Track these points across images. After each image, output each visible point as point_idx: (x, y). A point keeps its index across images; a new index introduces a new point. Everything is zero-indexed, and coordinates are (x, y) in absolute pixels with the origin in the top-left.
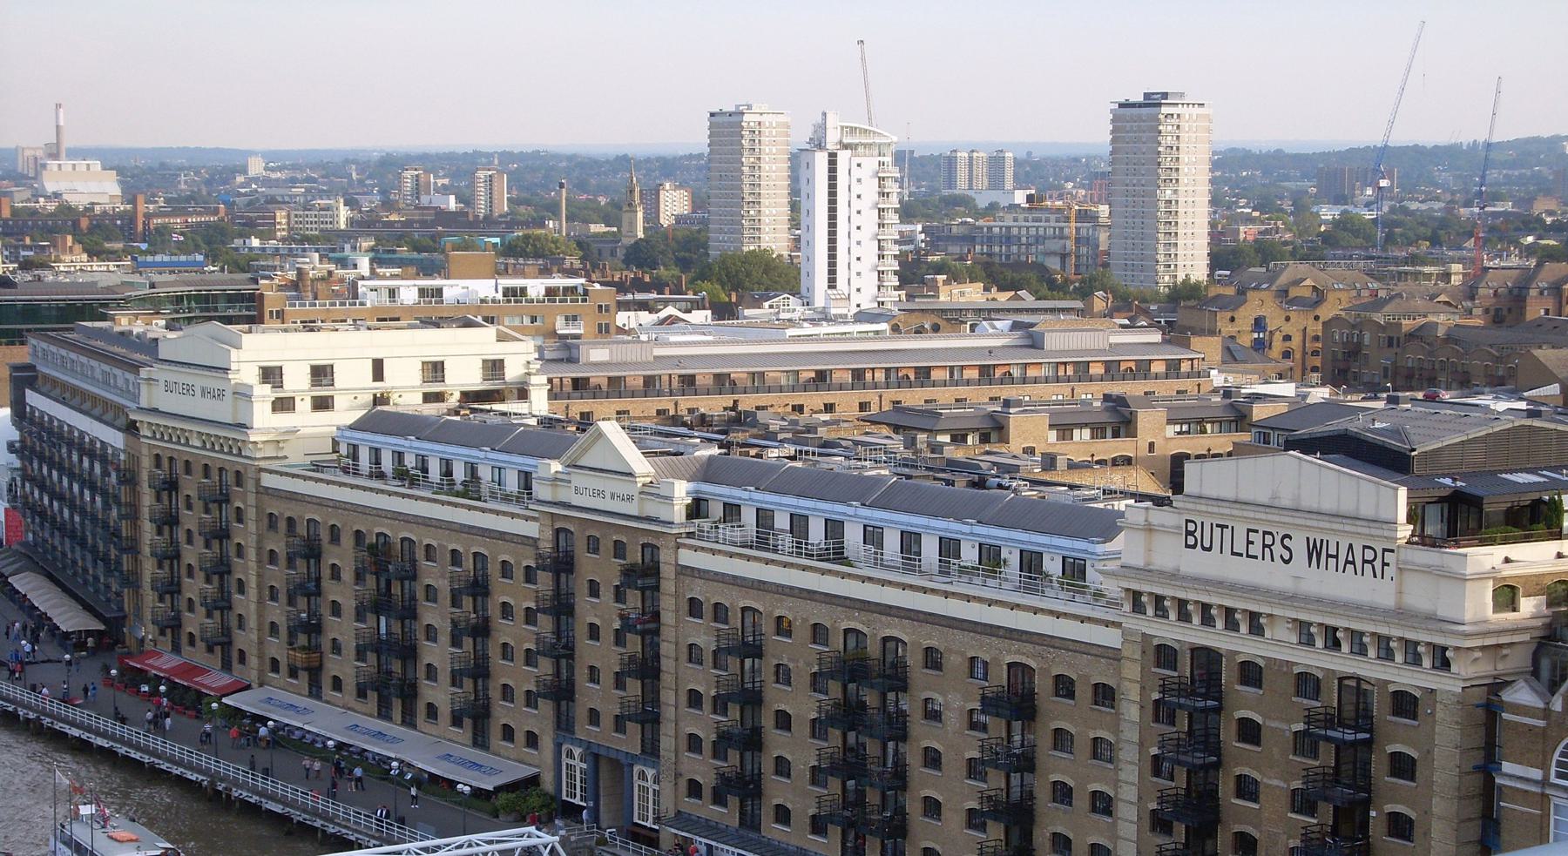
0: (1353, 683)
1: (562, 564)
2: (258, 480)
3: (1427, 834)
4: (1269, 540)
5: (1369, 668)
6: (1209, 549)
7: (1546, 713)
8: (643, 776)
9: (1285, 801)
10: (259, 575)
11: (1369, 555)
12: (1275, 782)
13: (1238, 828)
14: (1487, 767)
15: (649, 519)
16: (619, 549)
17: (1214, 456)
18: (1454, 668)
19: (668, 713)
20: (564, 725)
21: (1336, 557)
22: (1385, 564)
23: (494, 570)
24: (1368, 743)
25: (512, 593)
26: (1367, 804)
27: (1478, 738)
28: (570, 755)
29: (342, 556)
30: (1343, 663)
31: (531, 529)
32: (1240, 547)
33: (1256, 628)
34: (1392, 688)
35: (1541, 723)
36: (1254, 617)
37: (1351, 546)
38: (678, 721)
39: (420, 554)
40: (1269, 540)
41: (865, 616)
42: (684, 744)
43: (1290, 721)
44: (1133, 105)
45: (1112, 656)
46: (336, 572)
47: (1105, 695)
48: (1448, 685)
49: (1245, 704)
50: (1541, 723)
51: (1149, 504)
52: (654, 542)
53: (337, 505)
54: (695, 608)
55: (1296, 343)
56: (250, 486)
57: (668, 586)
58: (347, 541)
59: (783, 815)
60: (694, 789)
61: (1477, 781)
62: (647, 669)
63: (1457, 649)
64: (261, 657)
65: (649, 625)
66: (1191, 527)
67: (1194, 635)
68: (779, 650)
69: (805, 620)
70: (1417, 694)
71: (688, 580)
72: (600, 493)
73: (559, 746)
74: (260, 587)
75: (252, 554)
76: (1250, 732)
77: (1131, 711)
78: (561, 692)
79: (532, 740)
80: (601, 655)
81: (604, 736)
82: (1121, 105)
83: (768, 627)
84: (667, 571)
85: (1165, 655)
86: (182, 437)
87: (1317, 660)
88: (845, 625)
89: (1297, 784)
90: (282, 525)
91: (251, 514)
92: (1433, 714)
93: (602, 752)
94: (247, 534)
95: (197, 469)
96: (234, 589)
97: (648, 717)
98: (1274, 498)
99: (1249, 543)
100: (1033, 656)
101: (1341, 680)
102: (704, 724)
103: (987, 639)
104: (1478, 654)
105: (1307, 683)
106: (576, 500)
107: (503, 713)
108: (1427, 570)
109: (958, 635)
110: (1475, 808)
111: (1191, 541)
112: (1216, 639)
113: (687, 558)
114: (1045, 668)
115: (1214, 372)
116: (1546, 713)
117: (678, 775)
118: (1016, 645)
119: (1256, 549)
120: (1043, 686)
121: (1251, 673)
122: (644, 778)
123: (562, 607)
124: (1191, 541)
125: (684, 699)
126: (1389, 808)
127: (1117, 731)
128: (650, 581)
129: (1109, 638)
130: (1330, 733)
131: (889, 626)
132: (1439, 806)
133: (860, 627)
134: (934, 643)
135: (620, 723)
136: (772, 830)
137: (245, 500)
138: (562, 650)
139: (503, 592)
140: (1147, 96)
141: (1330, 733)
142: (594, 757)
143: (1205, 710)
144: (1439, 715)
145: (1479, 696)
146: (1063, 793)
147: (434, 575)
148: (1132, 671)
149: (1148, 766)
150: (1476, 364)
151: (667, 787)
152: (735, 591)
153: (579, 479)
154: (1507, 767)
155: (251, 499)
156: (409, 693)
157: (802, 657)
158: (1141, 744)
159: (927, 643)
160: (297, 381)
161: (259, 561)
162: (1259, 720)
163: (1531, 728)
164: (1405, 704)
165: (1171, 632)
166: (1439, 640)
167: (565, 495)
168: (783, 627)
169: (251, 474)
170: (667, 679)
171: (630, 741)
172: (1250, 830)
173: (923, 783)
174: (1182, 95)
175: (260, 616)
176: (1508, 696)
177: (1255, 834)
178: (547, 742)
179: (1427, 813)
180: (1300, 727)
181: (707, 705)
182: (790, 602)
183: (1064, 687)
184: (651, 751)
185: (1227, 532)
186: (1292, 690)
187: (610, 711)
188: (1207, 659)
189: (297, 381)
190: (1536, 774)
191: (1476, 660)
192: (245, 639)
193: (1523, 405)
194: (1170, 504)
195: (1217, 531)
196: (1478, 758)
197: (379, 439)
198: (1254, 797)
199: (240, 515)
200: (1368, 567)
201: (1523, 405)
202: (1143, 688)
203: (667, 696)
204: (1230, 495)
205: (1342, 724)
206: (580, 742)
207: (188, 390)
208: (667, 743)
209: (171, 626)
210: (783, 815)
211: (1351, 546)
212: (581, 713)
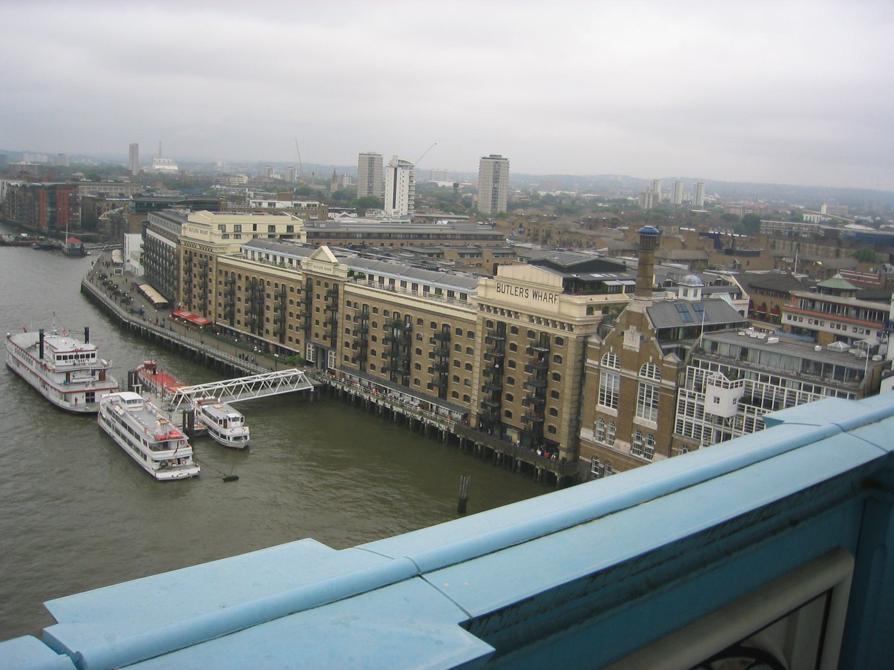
0: (544, 334)
1: (309, 289)
2: (217, 260)
3: (564, 379)
4: (522, 290)
5: (550, 330)
6: (504, 292)
7: (601, 344)
8: (331, 354)
9: (523, 368)
10: (216, 289)
11: (551, 296)
12: (520, 363)
13: (509, 376)
14: (583, 361)
15: (336, 276)
16: (327, 285)
17: (506, 265)
18: (574, 331)
19: (340, 335)
20: (308, 336)
21: (541, 296)
22: (555, 299)
23: (288, 289)
24: (548, 352)
25: (292, 297)
26: (547, 370)
27: (580, 352)
28: (309, 346)
29: (242, 283)
30: (542, 328)
31: (300, 278)
32: (513, 292)
33: (517, 317)
34: (556, 336)
35: (599, 348)
36: (516, 313)
37: (546, 294)
38: (343, 337)
39: (266, 284)
40: (522, 290)
41: (400, 308)
42: (344, 344)
43: (527, 345)
44: (487, 158)
45: (474, 323)
46: (239, 288)
47: (471, 335)
48: (573, 336)
49: (513, 339)
50: (599, 348)
51: (486, 278)
53: (241, 268)
54: (349, 303)
55: (532, 232)
56: (214, 261)
57: (341, 296)
58: (243, 279)
59: (373, 367)
60: (346, 358)
61: (579, 364)
62: (334, 323)
63: (575, 325)
64: (216, 313)
65: (334, 308)
66: (499, 286)
67: (498, 318)
68: (374, 317)
69: (382, 309)
70: (563, 338)
72: (322, 268)
73: (306, 344)
74: (216, 292)
75: (214, 282)
76: (514, 347)
77: (479, 340)
78: (307, 328)
79: (298, 341)
80: (320, 316)
81: (319, 341)
82: (483, 158)
83: (371, 310)
84: (341, 292)
85: (490, 323)
86: (194, 245)
87: (535, 327)
88: (394, 311)
89: (527, 363)
90: (224, 273)
91: (214, 269)
92: (567, 344)
93: (319, 346)
94: (212, 275)
95: (198, 255)
96: (208, 292)
97: (333, 337)
98: (524, 278)
99: (516, 291)
100: (451, 322)
101: (541, 333)
102: (350, 338)
103: (436, 317)
104: (581, 327)
105: (531, 334)
106: (314, 270)
107: (289, 333)
108: (568, 302)
109: (428, 316)
110: (579, 372)
111: (499, 290)
112: (505, 319)
113: (347, 288)
114: (454, 326)
115: (507, 240)
116: (601, 344)
117: (341, 354)
118: (445, 319)
119: (518, 293)
120: (452, 331)
121: (515, 330)
122: (331, 355)
123: (308, 302)
124: (499, 290)
125: (344, 331)
126: (554, 371)
127: (474, 346)
128: (336, 295)
129: (473, 318)
130: (537, 349)
131: (407, 311)
132: (568, 371)
133: (398, 311)
134: (421, 317)
135: (325, 338)
136: (370, 371)
137: (212, 265)
138: (308, 316)
139: (291, 296)
140: (491, 156)
141: (537, 349)
142: (316, 348)
143: (501, 341)
144: (569, 345)
145: (581, 339)
146: (457, 364)
147: (270, 290)
148: (479, 328)
149: (483, 356)
150: (584, 241)
151: (338, 357)
153: (315, 263)
154: (588, 361)
155: (215, 265)
156: (261, 327)
157: (380, 319)
158: (481, 350)
159: (418, 317)
160: (230, 229)
161: (216, 284)
162: (516, 344)
163: (596, 350)
164: (559, 341)
165: (491, 317)
166: (570, 323)
167: (310, 268)
168: (375, 310)
169: (215, 257)
170: (340, 325)
171: (327, 343)
172: (512, 376)
173: (416, 359)
174: (501, 156)
175: (216, 301)
176: (590, 340)
177: (514, 378)
178: (302, 342)
179: (565, 373)
180: (528, 346)
181: (351, 333)
182: (377, 303)
183: (459, 332)
184: (334, 345)
185: (510, 288)
186: (527, 336)
187: (322, 333)
188: (502, 325)
189: (230, 229)
190: (597, 363)
191: (581, 329)
192: (211, 308)
193: (597, 253)
194: (493, 278)
195: (506, 287)
196: (580, 357)
197: (254, 248)
198: (514, 367)
199: (211, 270)
200: (550, 300)
201: (597, 253)
202: (482, 333)
203: (340, 330)
204: (511, 277)
205: (541, 346)
206: (312, 343)
207: (196, 231)
208: (339, 344)
209: (188, 303)
210: (373, 367)
211: (546, 294)
212: (313, 334)
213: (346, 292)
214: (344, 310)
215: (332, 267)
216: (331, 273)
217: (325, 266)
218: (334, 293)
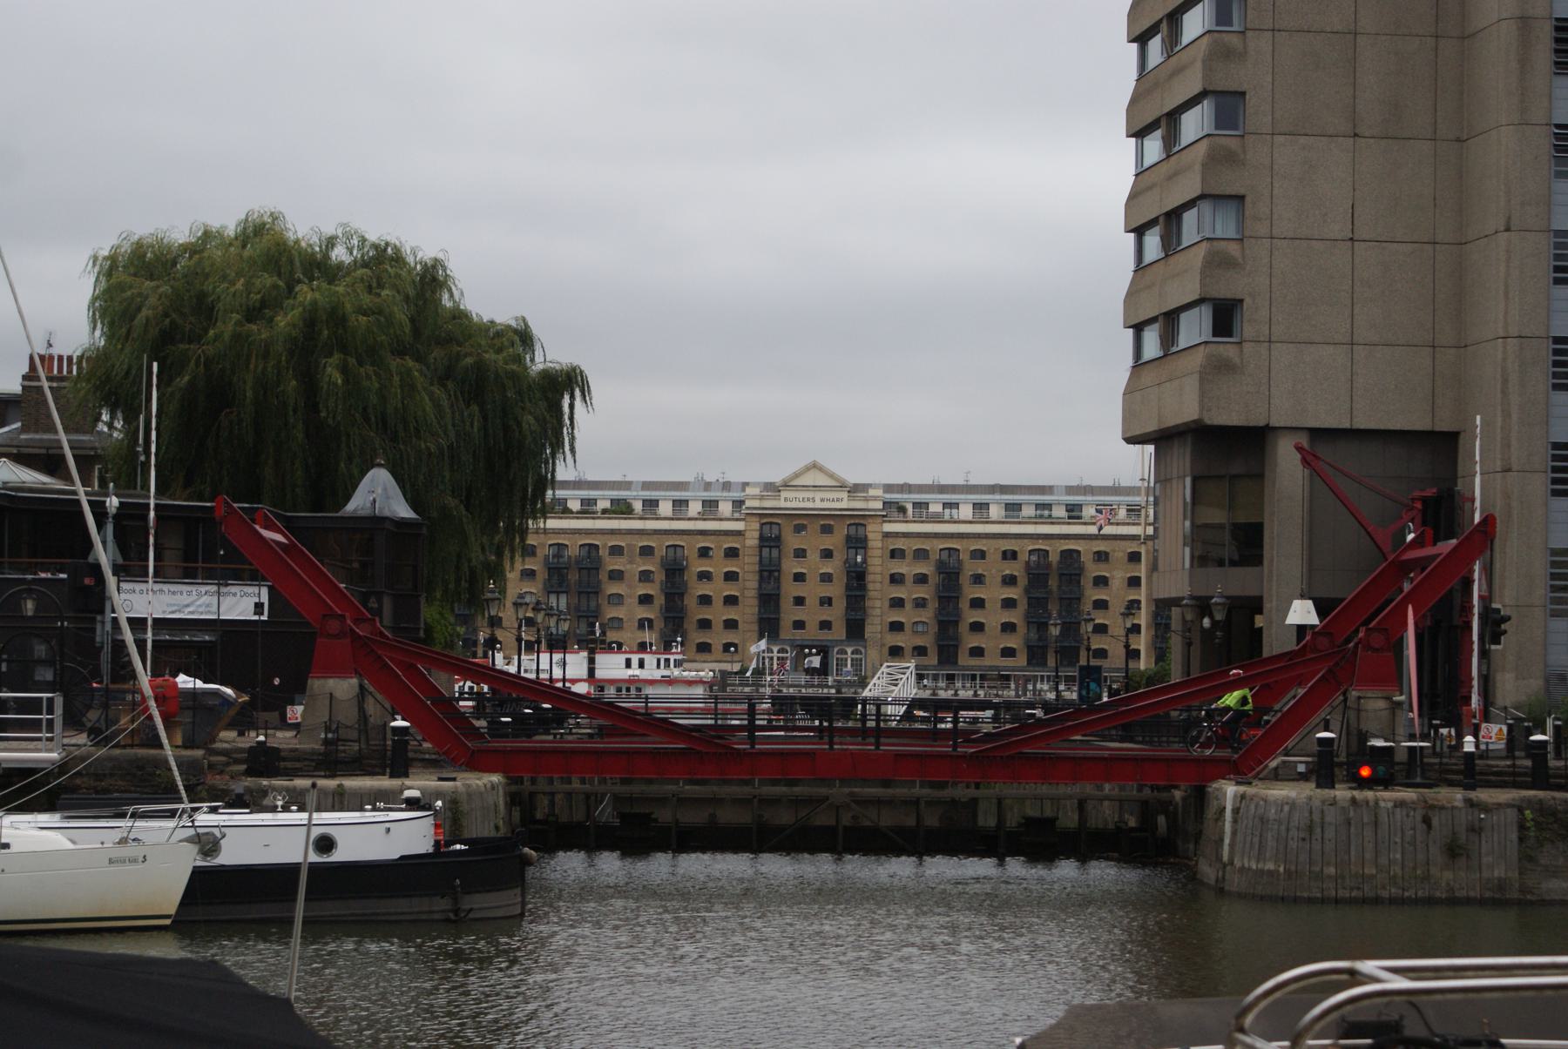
31: (739, 526)
52: (862, 522)
54: (895, 554)
69: (996, 549)
71: (890, 540)
106: (789, 505)
113: (888, 527)
131: (1067, 544)
152: (935, 541)
157: (994, 568)
168: (981, 555)
171: (839, 632)
182: (984, 541)
208: (874, 627)
213: (887, 535)
214: (878, 567)
215: (845, 495)
216: (844, 505)
217: (818, 495)
218: (857, 542)
